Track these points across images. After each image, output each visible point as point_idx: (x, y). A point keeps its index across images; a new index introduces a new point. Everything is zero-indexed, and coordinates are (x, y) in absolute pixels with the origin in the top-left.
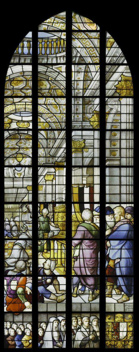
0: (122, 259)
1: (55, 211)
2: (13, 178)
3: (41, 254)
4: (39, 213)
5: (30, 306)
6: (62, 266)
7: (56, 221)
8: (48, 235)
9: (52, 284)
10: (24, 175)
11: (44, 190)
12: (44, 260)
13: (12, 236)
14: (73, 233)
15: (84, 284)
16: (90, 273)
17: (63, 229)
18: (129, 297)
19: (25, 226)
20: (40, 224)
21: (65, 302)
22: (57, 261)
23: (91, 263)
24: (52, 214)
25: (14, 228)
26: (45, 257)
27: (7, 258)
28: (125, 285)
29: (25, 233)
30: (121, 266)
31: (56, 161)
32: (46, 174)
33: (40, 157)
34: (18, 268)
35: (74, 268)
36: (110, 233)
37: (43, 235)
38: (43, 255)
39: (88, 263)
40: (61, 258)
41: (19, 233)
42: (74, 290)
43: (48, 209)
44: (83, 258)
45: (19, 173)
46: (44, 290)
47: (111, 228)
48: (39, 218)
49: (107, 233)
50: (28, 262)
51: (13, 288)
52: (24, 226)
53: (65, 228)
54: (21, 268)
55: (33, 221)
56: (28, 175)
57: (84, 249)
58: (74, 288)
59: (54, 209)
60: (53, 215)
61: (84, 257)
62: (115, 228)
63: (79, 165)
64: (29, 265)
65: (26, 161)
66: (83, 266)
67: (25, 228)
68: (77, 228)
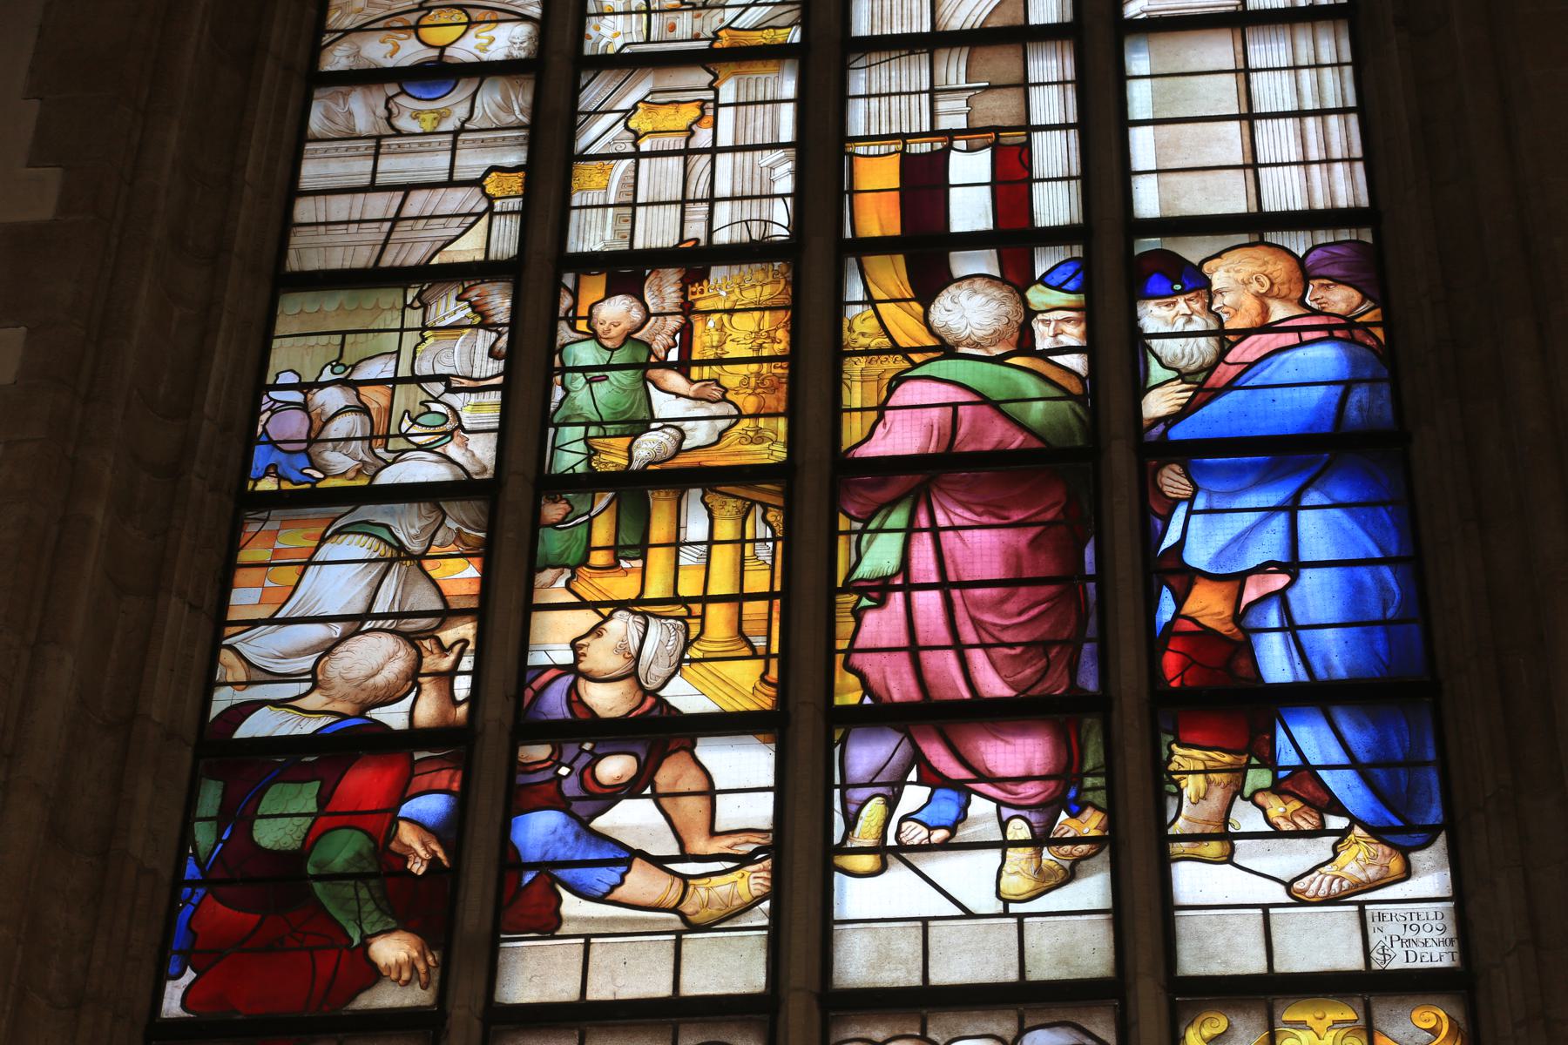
0: (1308, 576)
1: (701, 305)
2: (379, 138)
3: (561, 583)
4: (563, 327)
5: (421, 966)
6: (746, 652)
7: (702, 363)
8: (630, 450)
9: (648, 791)
10: (469, 119)
11: (622, 183)
12: (585, 620)
13: (318, 475)
14: (853, 428)
15: (955, 770)
16: (1011, 685)
17: (759, 407)
18: (1404, 852)
19: (435, 407)
20: (564, 388)
21: (765, 922)
22: (703, 617)
23: (1020, 614)
24: (674, 323)
25: (342, 427)
26: (590, 596)
27: (254, 624)
28: (1354, 764)
29: (431, 451)
30: (1299, 620)
31: (728, 26)
32: (642, 101)
33: (601, 14)
34: (340, 688)
35: (857, 660)
36: (1184, 406)
37: (591, 452)
38: (579, 587)
39: (988, 618)
40: (738, 598)
41: (380, 451)
42: (851, 823)
43: (640, 297)
44: (944, 585)
45: (432, 111)
46: (571, 839)
47: (1182, 376)
48: (560, 351)
49: (1157, 404)
50: (439, 642)
51: (272, 834)
52: (430, 411)
53: (777, 401)
54: (371, 681)
55: (506, 373)
56: (502, 115)
57: (954, 528)
58: (853, 808)
59: (691, 298)
60: (686, 332)
61: (952, 577)
62: (1224, 373)
63: (906, 30)
64: (446, 663)
65: (492, 40)
66: (943, 637)
67: (439, 420)
68: (891, 391)
